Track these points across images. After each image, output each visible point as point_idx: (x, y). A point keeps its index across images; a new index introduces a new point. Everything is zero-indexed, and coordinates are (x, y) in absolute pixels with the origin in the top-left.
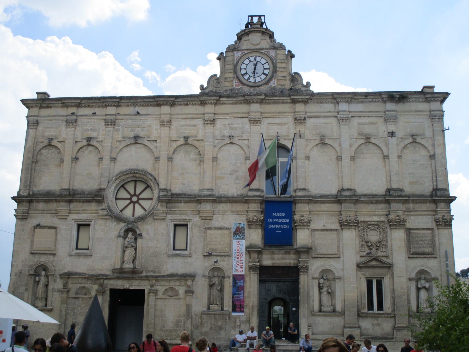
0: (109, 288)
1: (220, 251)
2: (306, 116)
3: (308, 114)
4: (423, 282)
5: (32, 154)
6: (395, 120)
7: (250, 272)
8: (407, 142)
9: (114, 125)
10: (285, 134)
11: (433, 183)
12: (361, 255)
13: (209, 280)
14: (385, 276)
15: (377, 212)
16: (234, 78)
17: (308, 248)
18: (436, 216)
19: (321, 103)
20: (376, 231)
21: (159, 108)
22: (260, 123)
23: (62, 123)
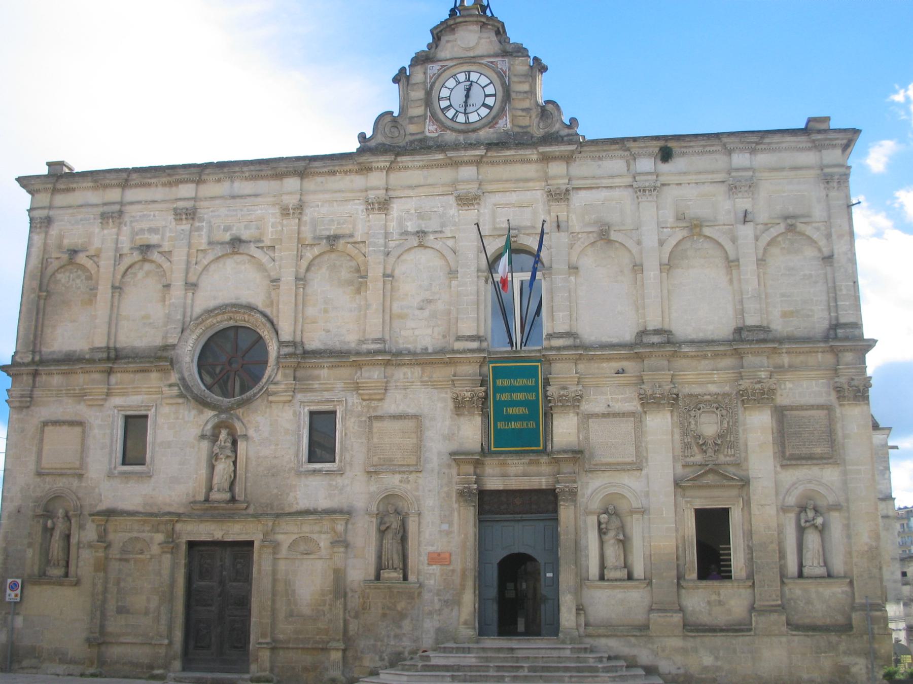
0: (185, 539)
1: (400, 463)
3: (576, 183)
4: (811, 514)
5: (39, 282)
6: (751, 189)
8: (774, 232)
9: (193, 219)
10: (529, 224)
11: (830, 314)
13: (379, 521)
14: (734, 505)
15: (716, 376)
17: (574, 452)
18: (837, 379)
19: (600, 158)
20: (714, 415)
21: (278, 182)
22: (479, 204)
23: (95, 219)
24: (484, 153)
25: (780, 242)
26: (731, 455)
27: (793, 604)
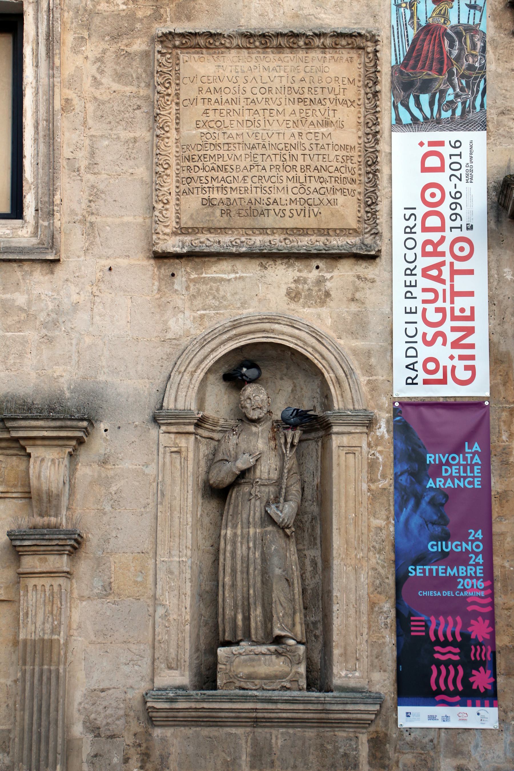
1: (289, 223)
13: (204, 450)
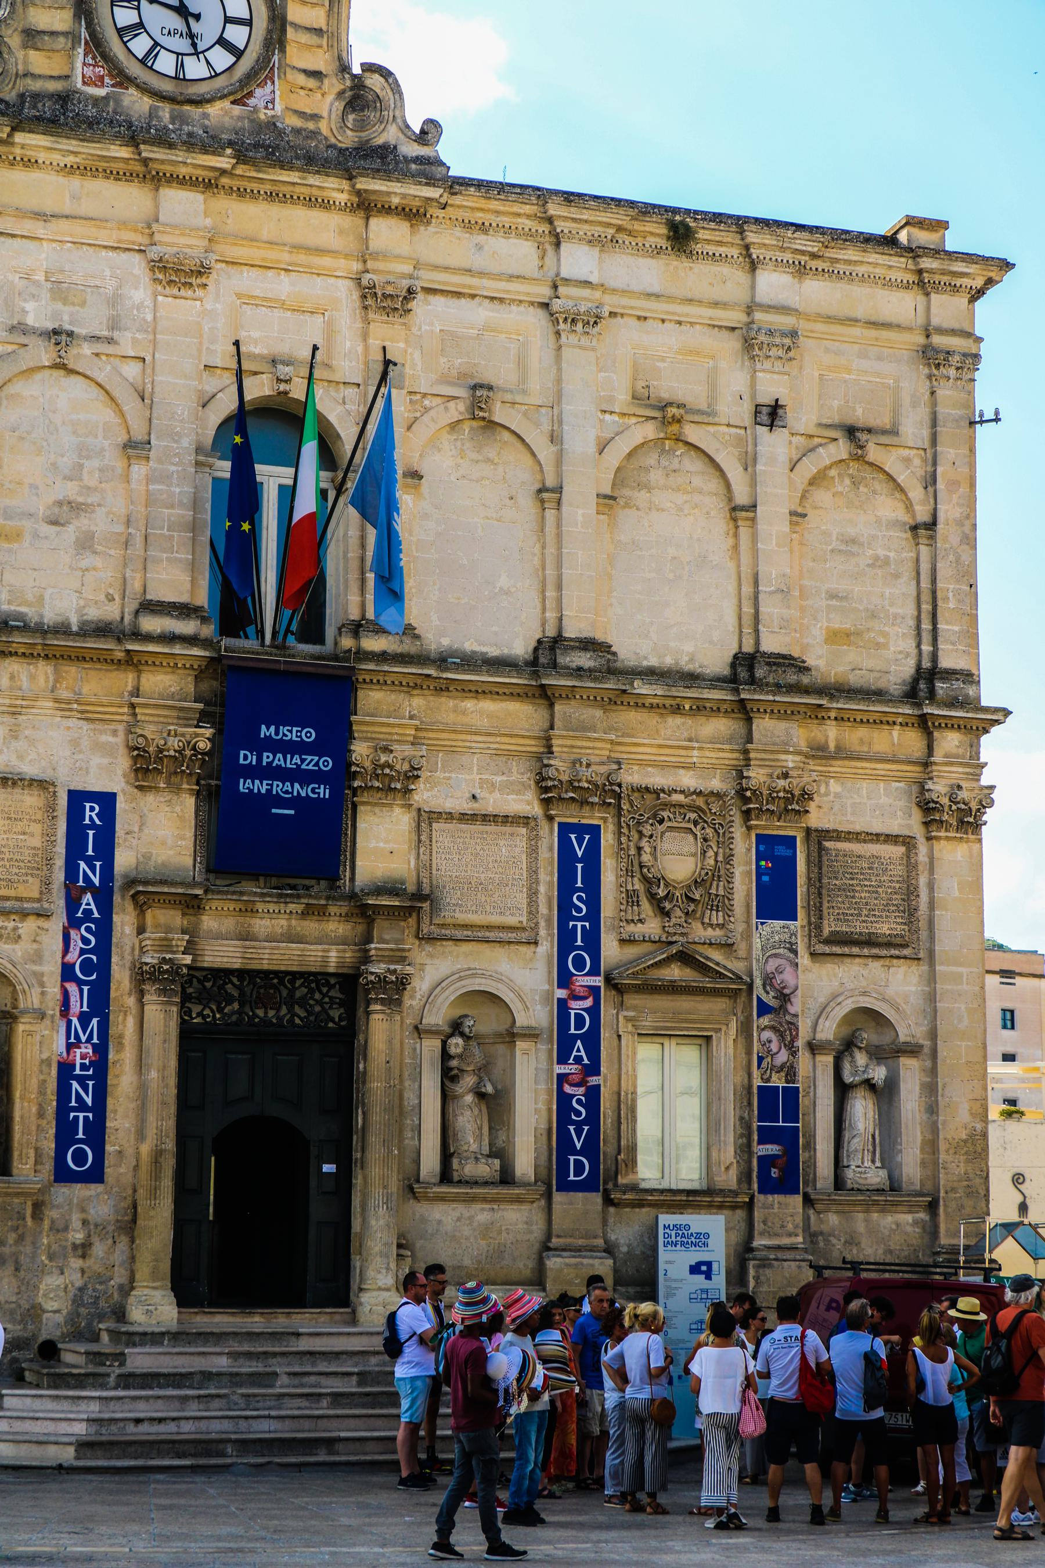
2: (418, 284)
3: (428, 278)
4: (861, 1059)
6: (791, 354)
7: (142, 993)
11: (919, 646)
12: (625, 936)
15: (695, 753)
16: (75, 39)
19: (484, 229)
20: (691, 837)
24: (228, 166)
25: (833, 478)
26: (718, 925)
27: (822, 1244)
